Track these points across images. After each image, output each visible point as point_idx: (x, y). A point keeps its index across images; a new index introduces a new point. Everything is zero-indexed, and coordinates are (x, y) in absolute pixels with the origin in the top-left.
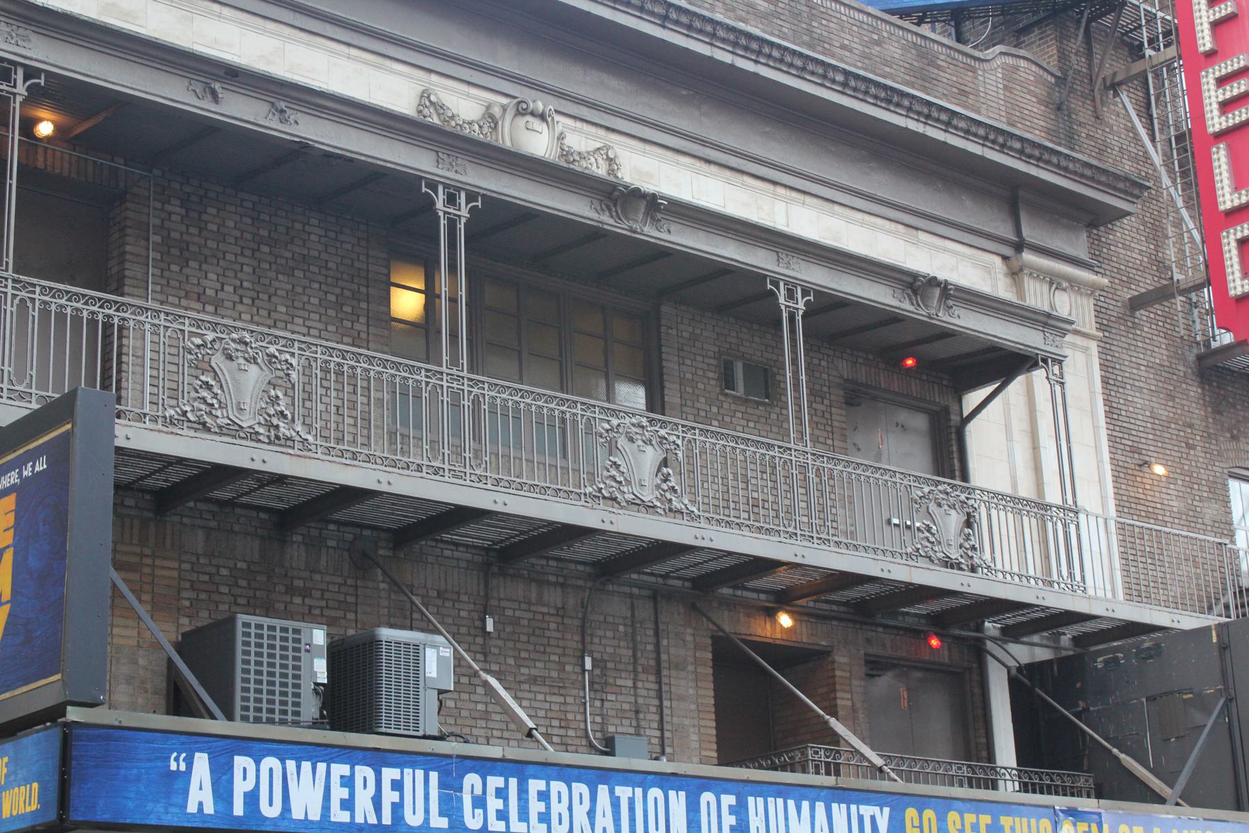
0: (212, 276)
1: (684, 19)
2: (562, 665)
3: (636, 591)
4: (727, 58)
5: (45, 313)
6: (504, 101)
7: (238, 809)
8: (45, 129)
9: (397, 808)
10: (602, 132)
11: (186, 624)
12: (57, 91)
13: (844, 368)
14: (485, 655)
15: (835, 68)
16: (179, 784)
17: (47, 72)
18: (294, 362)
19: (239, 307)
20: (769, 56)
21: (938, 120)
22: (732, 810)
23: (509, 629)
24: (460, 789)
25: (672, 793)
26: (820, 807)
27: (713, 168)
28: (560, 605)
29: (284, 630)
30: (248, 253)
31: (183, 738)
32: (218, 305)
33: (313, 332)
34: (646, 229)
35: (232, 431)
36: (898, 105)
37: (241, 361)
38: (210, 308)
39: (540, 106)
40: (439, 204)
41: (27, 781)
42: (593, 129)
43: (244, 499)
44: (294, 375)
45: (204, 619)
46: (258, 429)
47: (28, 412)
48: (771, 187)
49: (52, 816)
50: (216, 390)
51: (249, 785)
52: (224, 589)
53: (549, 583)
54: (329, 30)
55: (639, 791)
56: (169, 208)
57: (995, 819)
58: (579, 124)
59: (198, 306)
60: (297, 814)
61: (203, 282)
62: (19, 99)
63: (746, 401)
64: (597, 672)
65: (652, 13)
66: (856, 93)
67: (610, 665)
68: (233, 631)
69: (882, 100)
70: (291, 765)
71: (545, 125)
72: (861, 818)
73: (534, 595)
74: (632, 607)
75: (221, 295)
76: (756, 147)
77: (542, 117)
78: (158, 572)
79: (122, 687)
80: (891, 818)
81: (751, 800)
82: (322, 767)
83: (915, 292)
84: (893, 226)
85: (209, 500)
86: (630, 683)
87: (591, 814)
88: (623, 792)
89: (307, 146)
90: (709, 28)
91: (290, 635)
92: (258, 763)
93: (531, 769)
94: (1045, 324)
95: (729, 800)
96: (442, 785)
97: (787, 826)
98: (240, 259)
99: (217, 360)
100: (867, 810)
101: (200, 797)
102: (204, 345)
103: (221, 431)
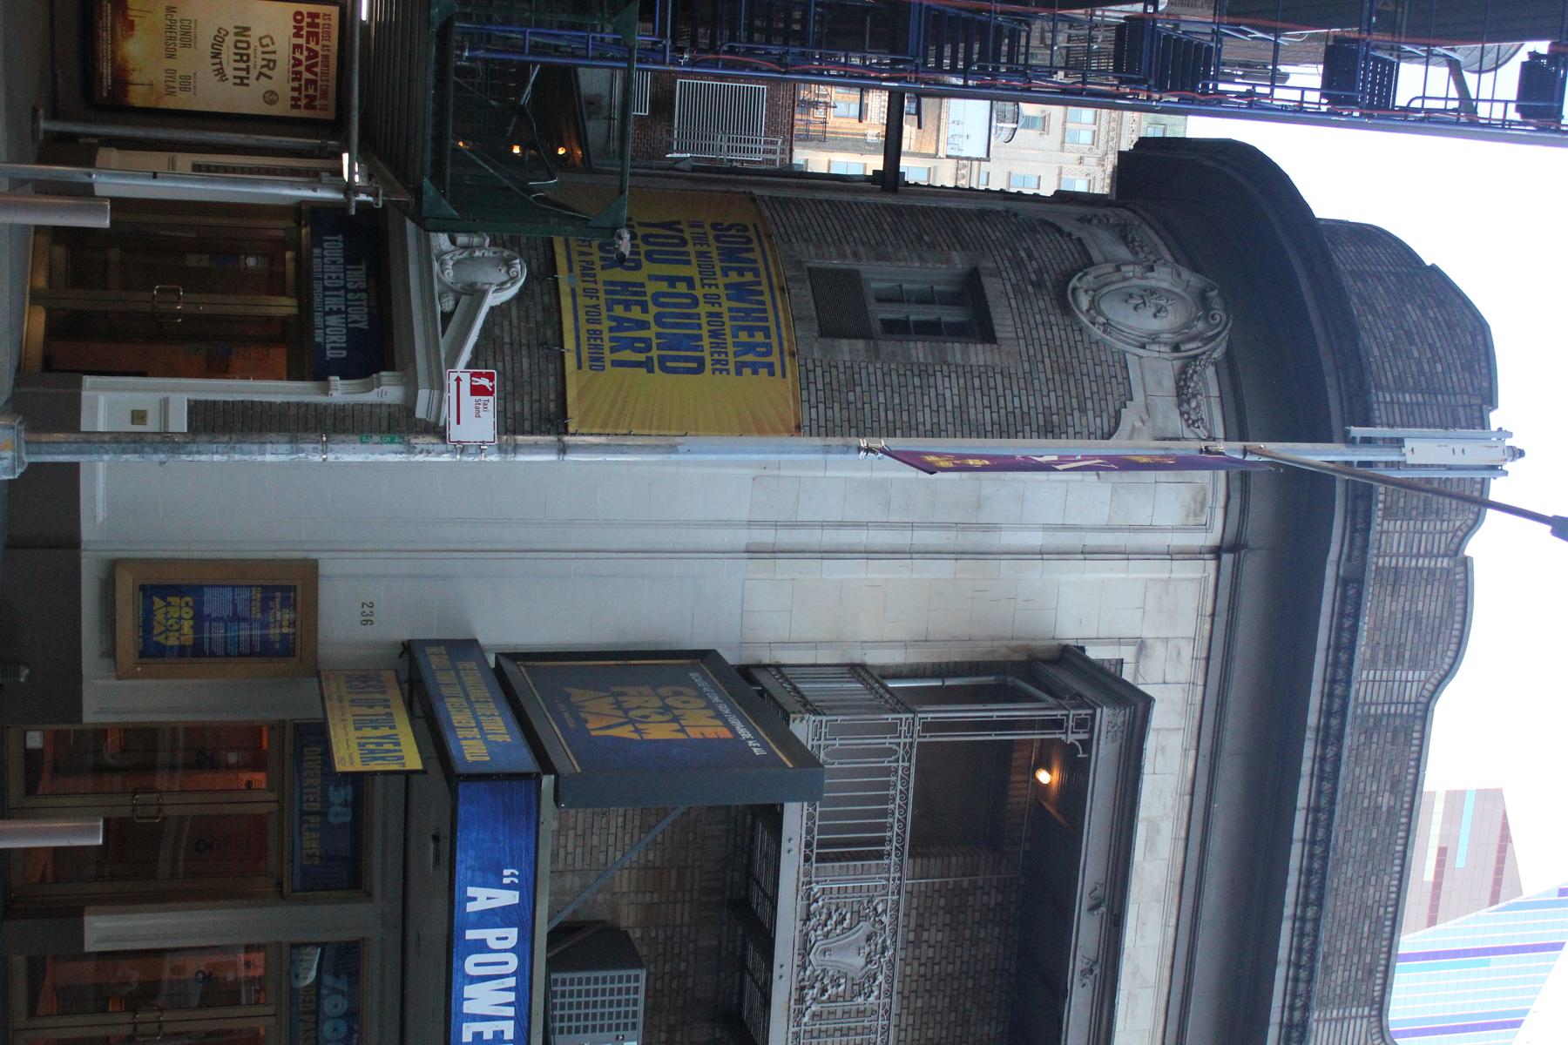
0: (940, 937)
5: (886, 772)
7: (471, 934)
8: (1044, 777)
11: (636, 934)
12: (1074, 791)
16: (491, 878)
17: (1089, 759)
18: (872, 999)
19: (916, 964)
29: (635, 1014)
30: (965, 968)
31: (531, 879)
32: (916, 944)
33: (903, 1034)
35: (805, 948)
37: (867, 950)
38: (911, 936)
41: (490, 753)
43: (748, 978)
44: (860, 1000)
45: (644, 951)
46: (810, 969)
47: (802, 739)
49: (461, 769)
50: (839, 928)
51: (493, 944)
52: (667, 968)
56: (993, 892)
59: (912, 925)
60: (469, 991)
61: (933, 931)
62: (1063, 737)
68: (632, 967)
70: (512, 982)
75: (924, 946)
78: (679, 906)
79: (577, 881)
82: (510, 1011)
85: (745, 947)
91: (630, 1020)
92: (512, 950)
98: (958, 961)
99: (865, 927)
101: (482, 898)
102: (877, 915)
103: (805, 937)
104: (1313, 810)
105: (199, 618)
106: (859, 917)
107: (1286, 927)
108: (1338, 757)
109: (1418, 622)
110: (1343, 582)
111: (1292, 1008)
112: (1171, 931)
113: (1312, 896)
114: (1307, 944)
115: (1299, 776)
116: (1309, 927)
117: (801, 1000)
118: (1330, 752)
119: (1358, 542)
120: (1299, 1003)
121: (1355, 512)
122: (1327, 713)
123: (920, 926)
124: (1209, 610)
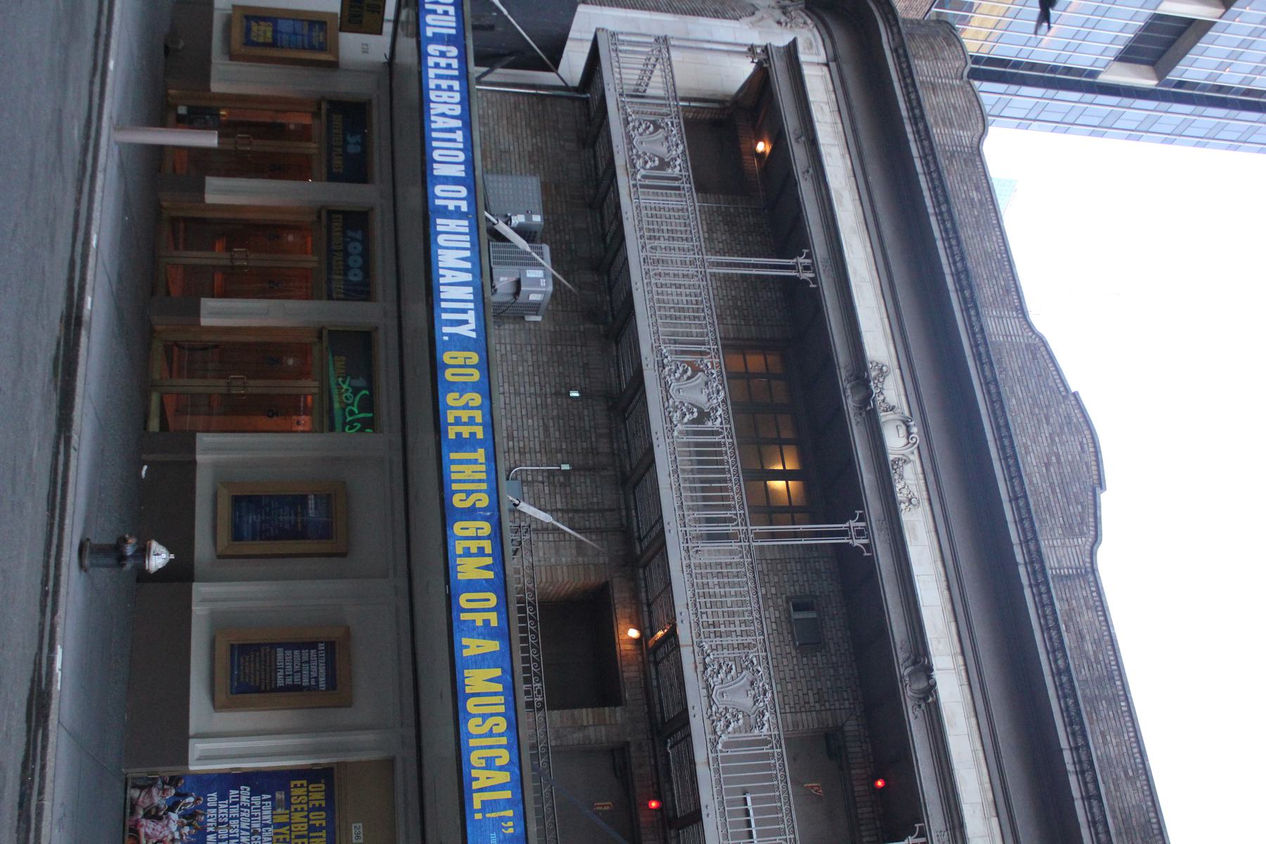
1: (1023, 511)
2: (561, 451)
3: (624, 513)
4: (1019, 558)
6: (907, 414)
8: (761, 147)
9: (434, 12)
10: (925, 496)
13: (851, 727)
14: (557, 394)
15: (1065, 656)
20: (1040, 594)
21: (1086, 784)
22: (458, 208)
23: (575, 412)
24: (448, 45)
25: (462, 167)
26: (468, 277)
27: (946, 593)
28: (600, 450)
34: (850, 401)
36: (1074, 734)
39: (914, 430)
40: (801, 260)
42: (924, 488)
48: (958, 650)
53: (612, 443)
54: (890, 304)
55: (461, 146)
57: (481, 443)
58: (921, 476)
63: (789, 618)
64: (562, 479)
65: (1013, 487)
66: (1059, 687)
67: (568, 490)
69: (1069, 716)
71: (904, 441)
72: (465, 311)
73: (600, 431)
74: (611, 510)
76: (980, 632)
77: (909, 433)
80: (469, 338)
81: (466, 223)
83: (915, 663)
84: (988, 786)
86: (559, 506)
87: (443, 115)
88: (459, 136)
89: (796, 185)
90: (1030, 535)
93: (465, 83)
94: (953, 829)
95: (464, 208)
96: (449, 35)
97: (452, 248)
100: (471, 316)
104: (923, 157)
105: (275, 31)
106: (657, 127)
107: (933, 220)
108: (926, 127)
109: (955, 109)
110: (895, 51)
111: (955, 263)
112: (869, 249)
113: (941, 199)
114: (949, 225)
115: (907, 141)
116: (946, 216)
117: (634, 166)
118: (921, 126)
119: (895, 30)
120: (958, 259)
121: (888, 20)
122: (911, 109)
123: (710, 231)
124: (831, 87)
